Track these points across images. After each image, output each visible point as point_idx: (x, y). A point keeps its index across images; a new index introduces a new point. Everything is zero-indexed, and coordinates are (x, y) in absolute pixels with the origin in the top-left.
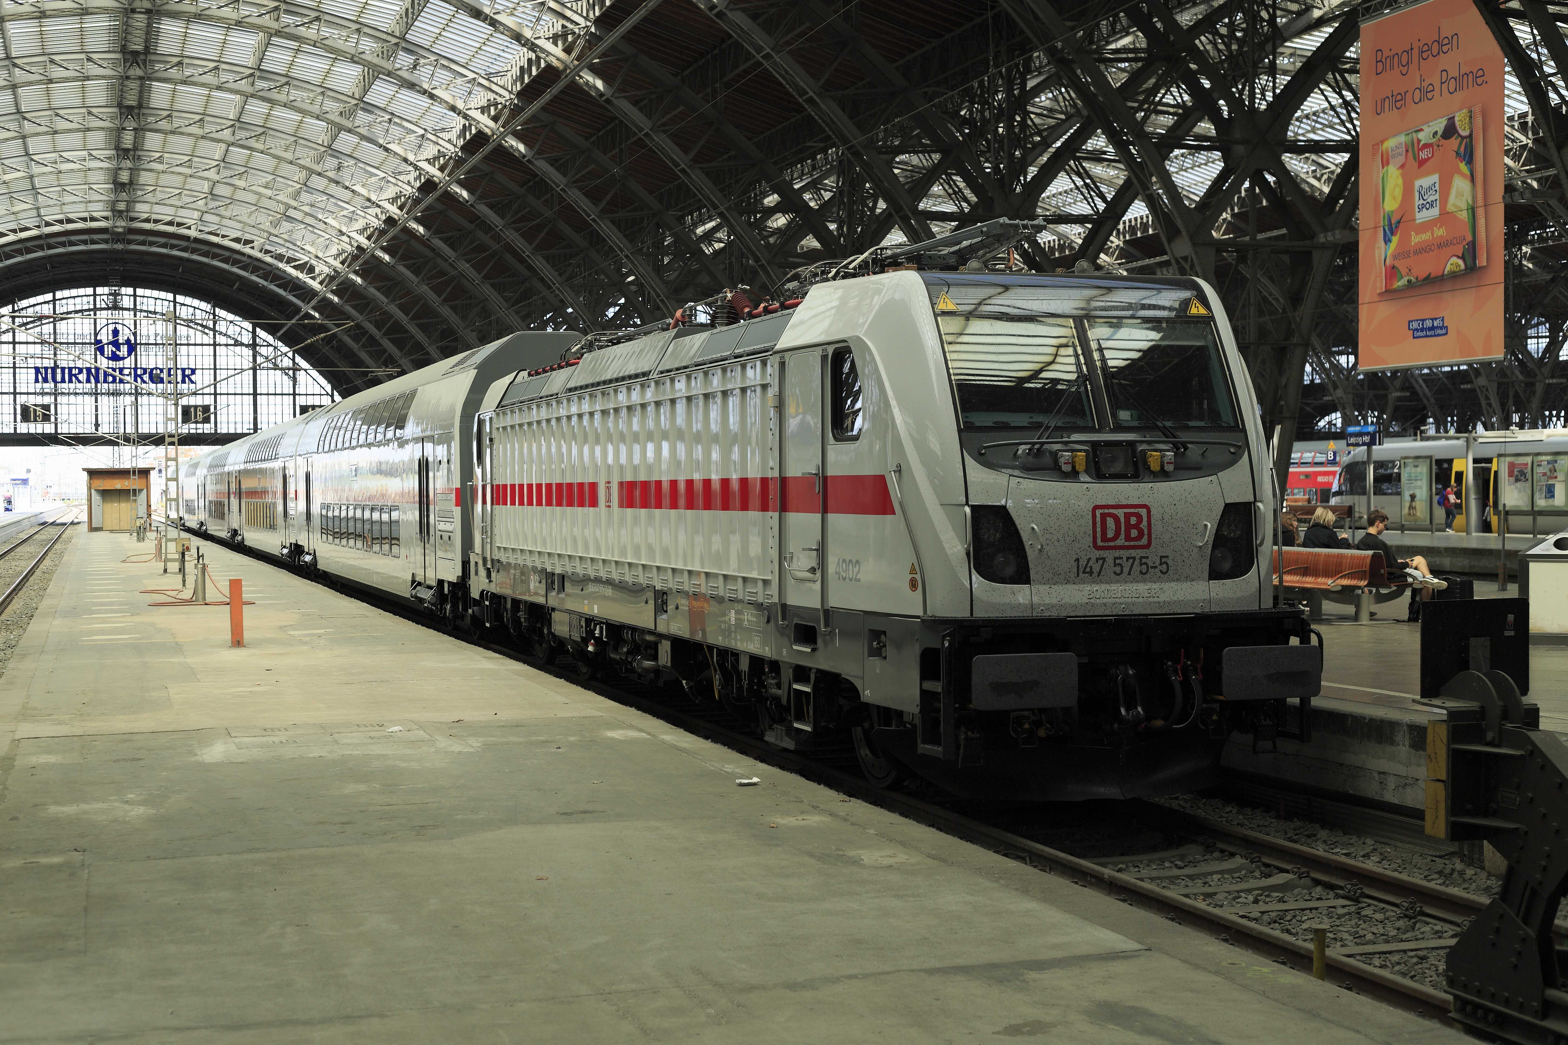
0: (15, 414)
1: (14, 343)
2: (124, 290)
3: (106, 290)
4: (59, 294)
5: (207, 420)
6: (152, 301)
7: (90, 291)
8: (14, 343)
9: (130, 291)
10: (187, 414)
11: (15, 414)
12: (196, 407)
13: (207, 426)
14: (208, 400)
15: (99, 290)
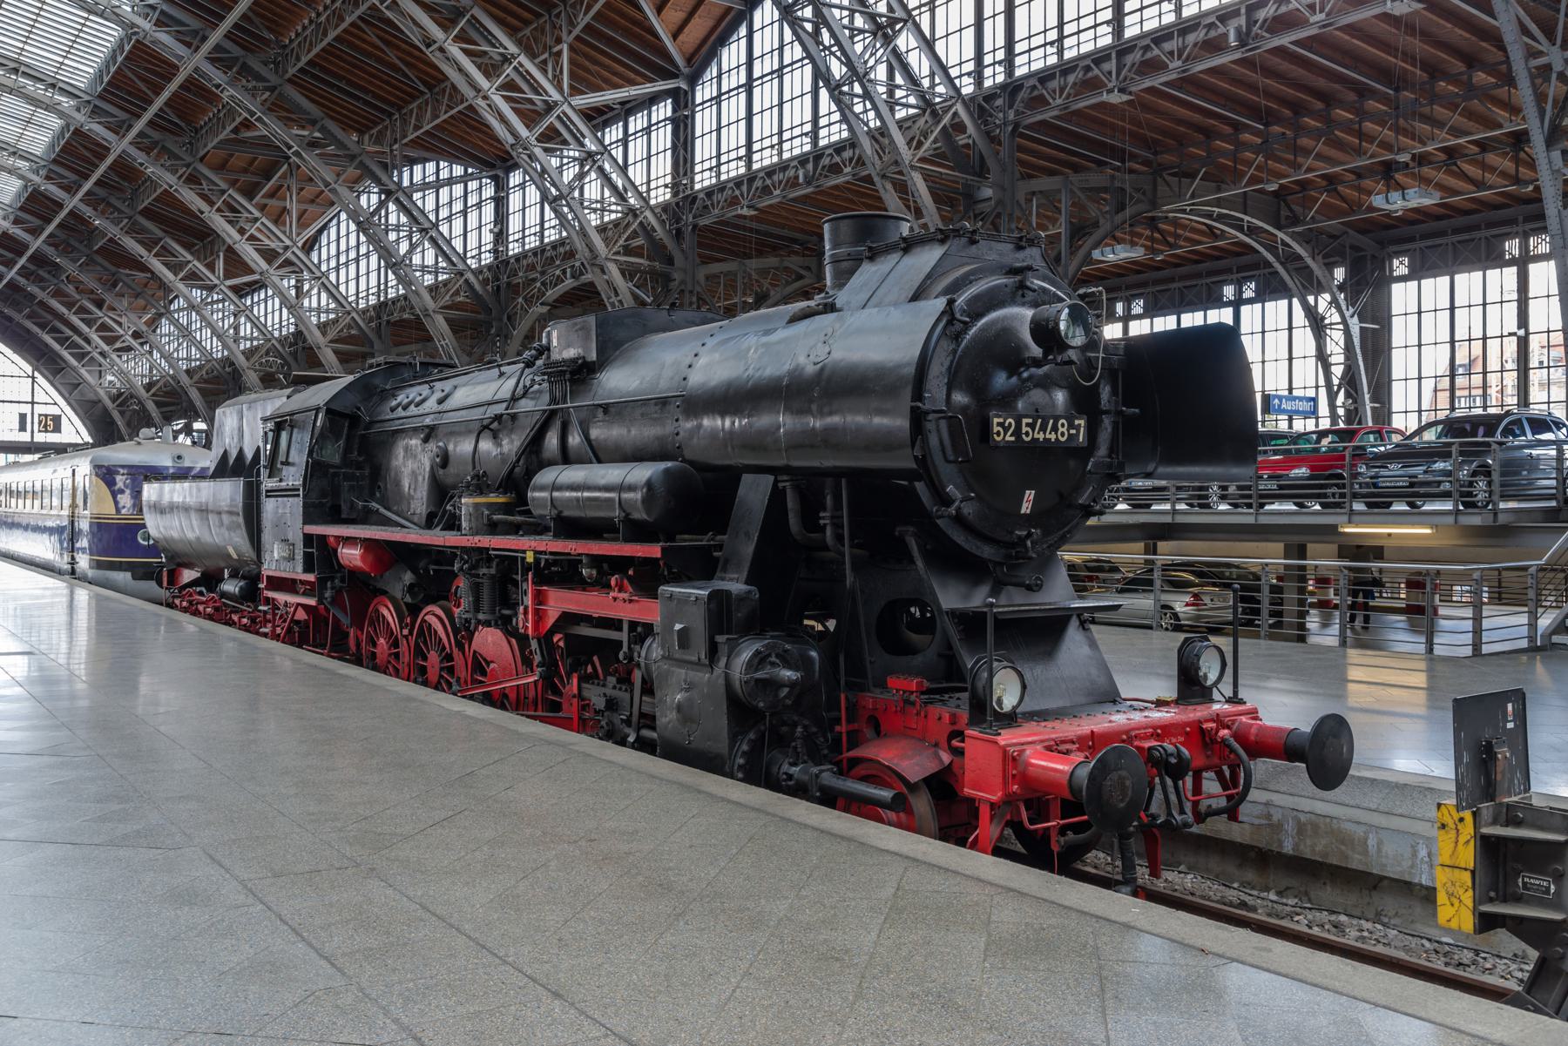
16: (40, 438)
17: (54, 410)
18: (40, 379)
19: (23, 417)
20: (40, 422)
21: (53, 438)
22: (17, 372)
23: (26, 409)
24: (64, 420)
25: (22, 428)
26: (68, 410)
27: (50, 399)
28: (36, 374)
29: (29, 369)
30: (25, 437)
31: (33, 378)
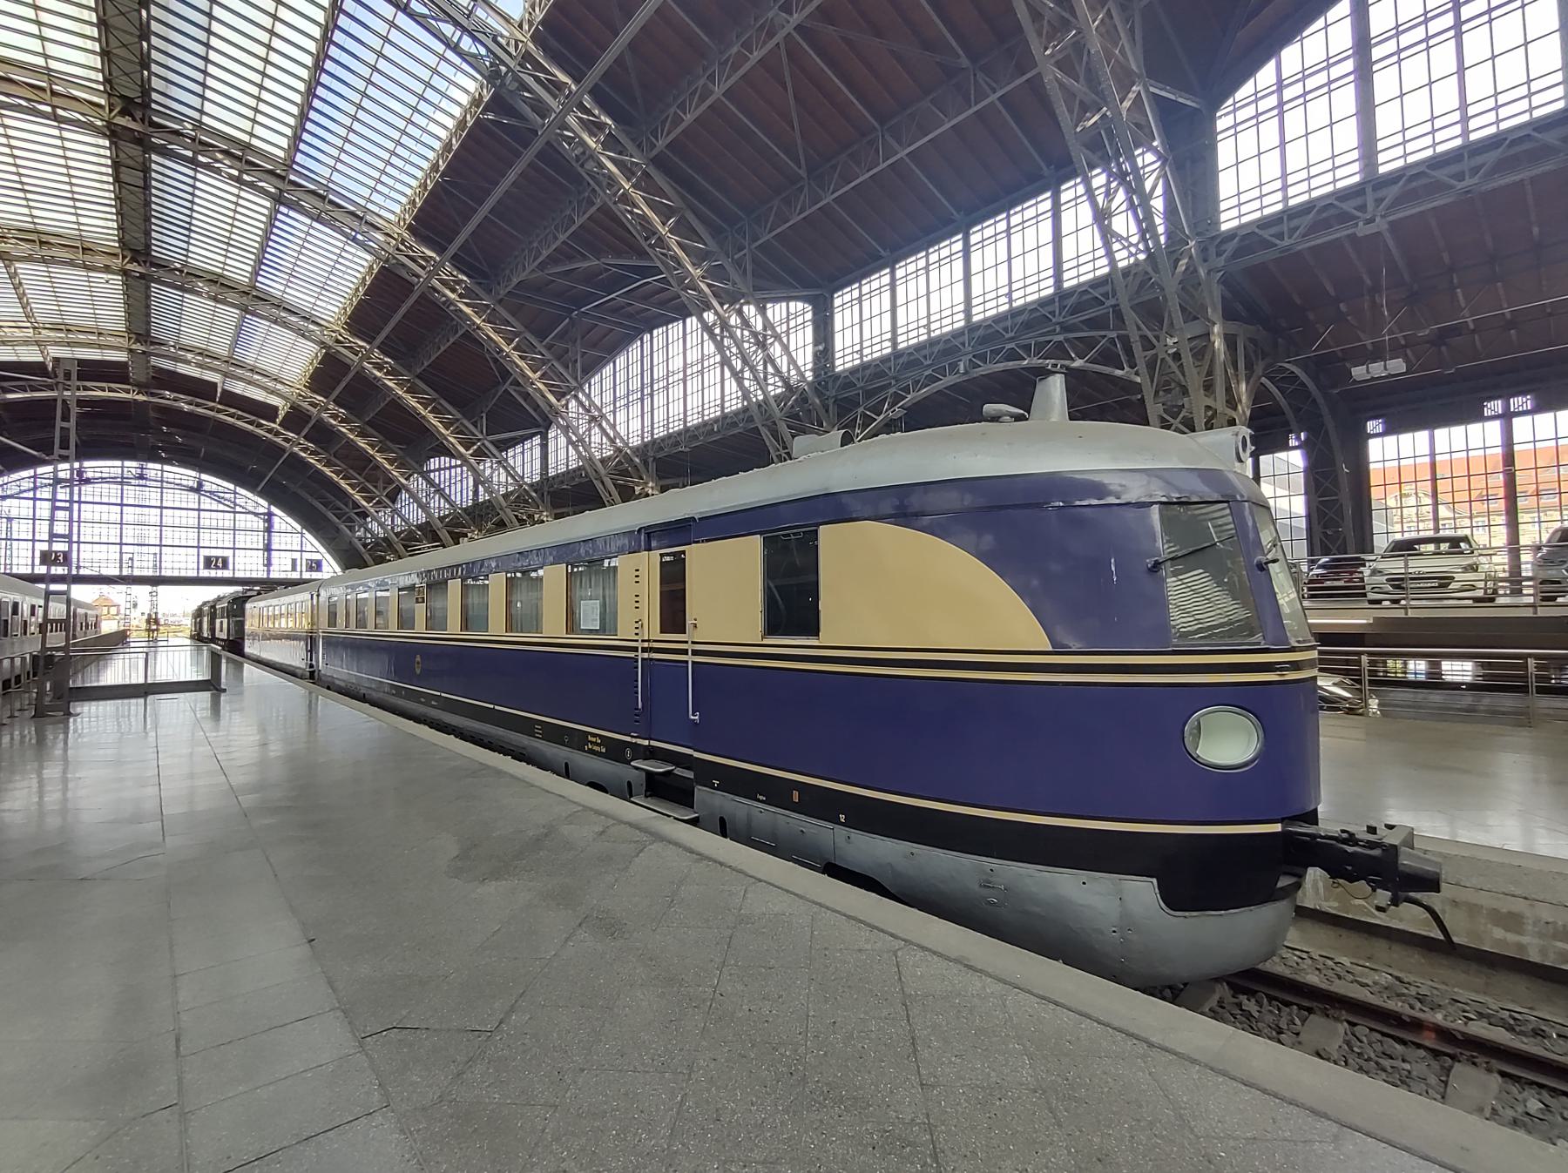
0: (33, 557)
1: (35, 499)
2: (151, 465)
3: (134, 464)
4: (86, 464)
5: (225, 566)
6: (178, 476)
7: (118, 463)
8: (35, 499)
9: (158, 466)
10: (208, 562)
11: (33, 557)
12: (217, 558)
13: (225, 571)
14: (228, 553)
15: (127, 463)
16: (306, 576)
17: (316, 557)
18: (308, 535)
19: (294, 561)
20: (307, 564)
21: (315, 575)
22: (289, 529)
23: (297, 555)
24: (324, 563)
25: (294, 569)
26: (328, 556)
27: (314, 547)
28: (304, 531)
29: (298, 527)
30: (295, 575)
31: (302, 533)
